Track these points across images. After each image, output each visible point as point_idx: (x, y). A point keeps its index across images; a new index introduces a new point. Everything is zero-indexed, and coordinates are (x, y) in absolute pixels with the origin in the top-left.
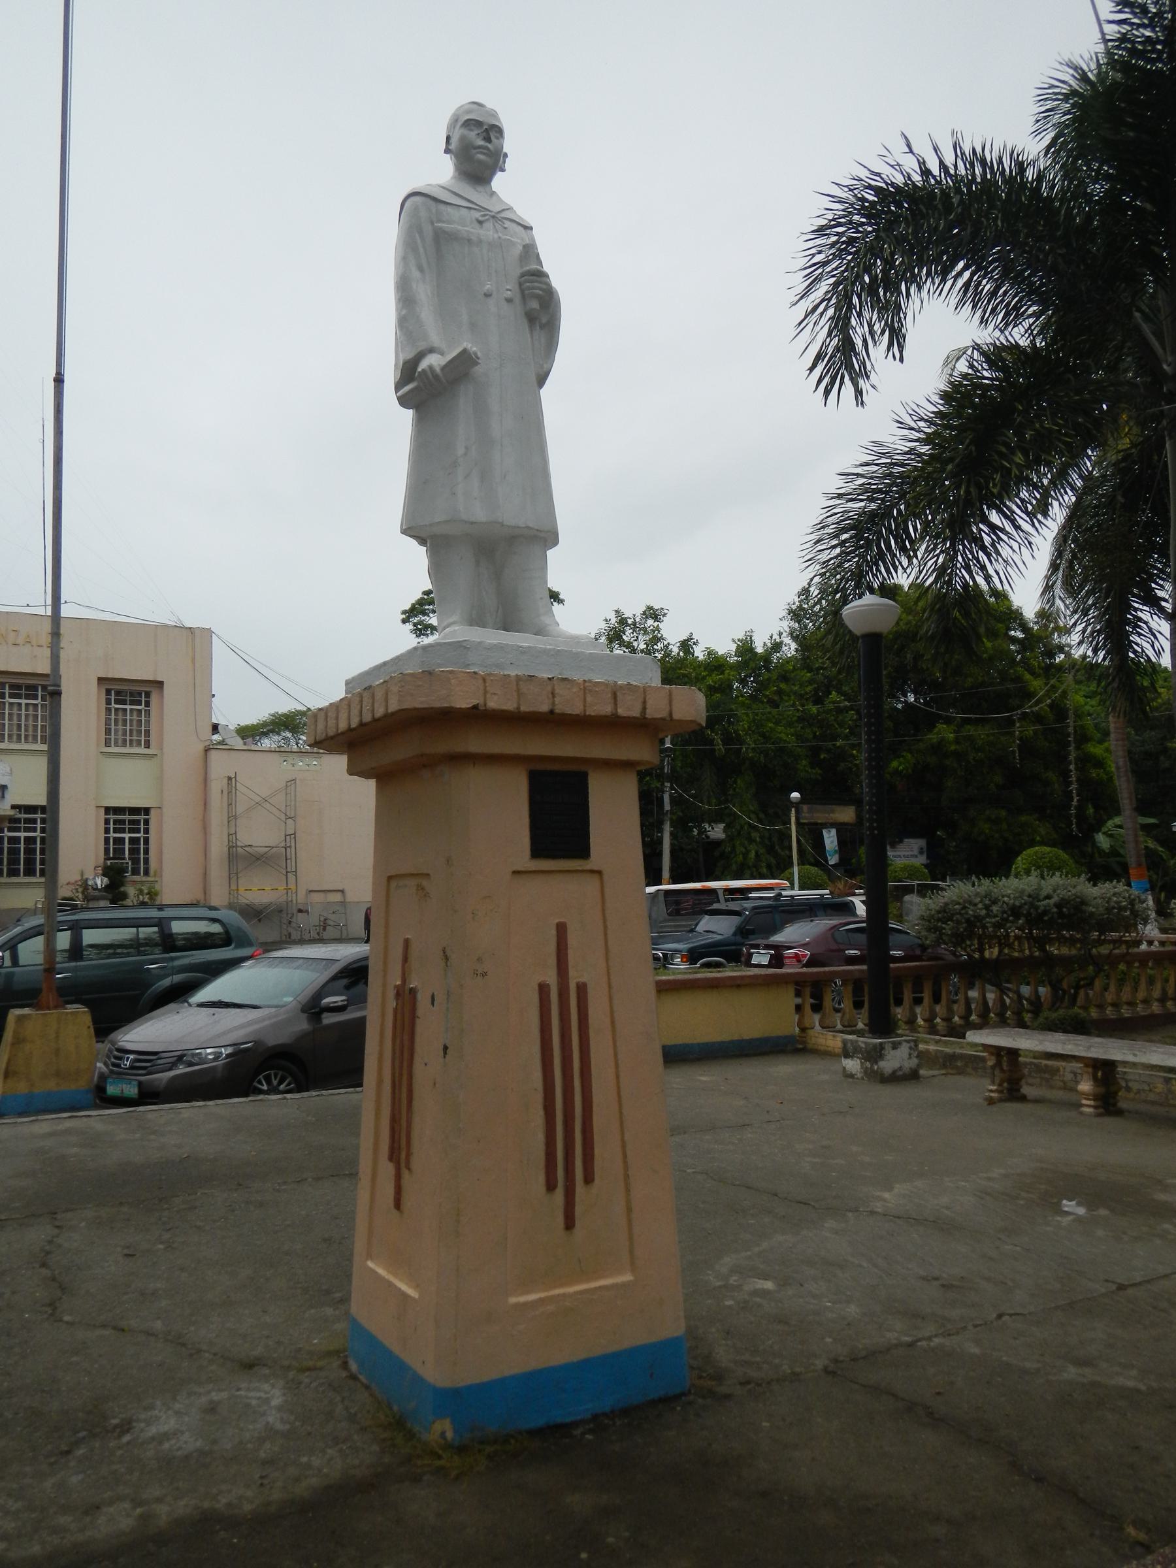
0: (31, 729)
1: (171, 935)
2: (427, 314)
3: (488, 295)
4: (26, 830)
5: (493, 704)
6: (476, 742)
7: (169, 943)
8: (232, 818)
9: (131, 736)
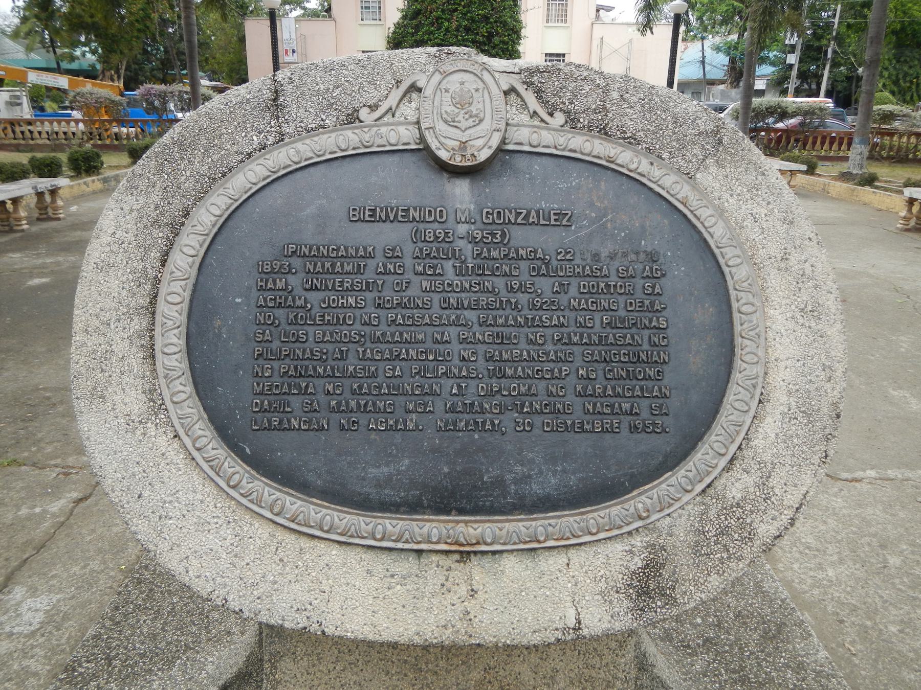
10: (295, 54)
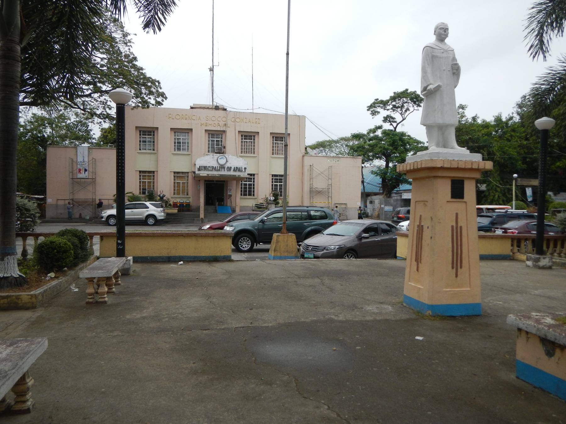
1: (311, 215)
2: (429, 75)
3: (444, 70)
5: (445, 166)
6: (440, 174)
7: (310, 217)
8: (311, 179)
10: (87, 173)
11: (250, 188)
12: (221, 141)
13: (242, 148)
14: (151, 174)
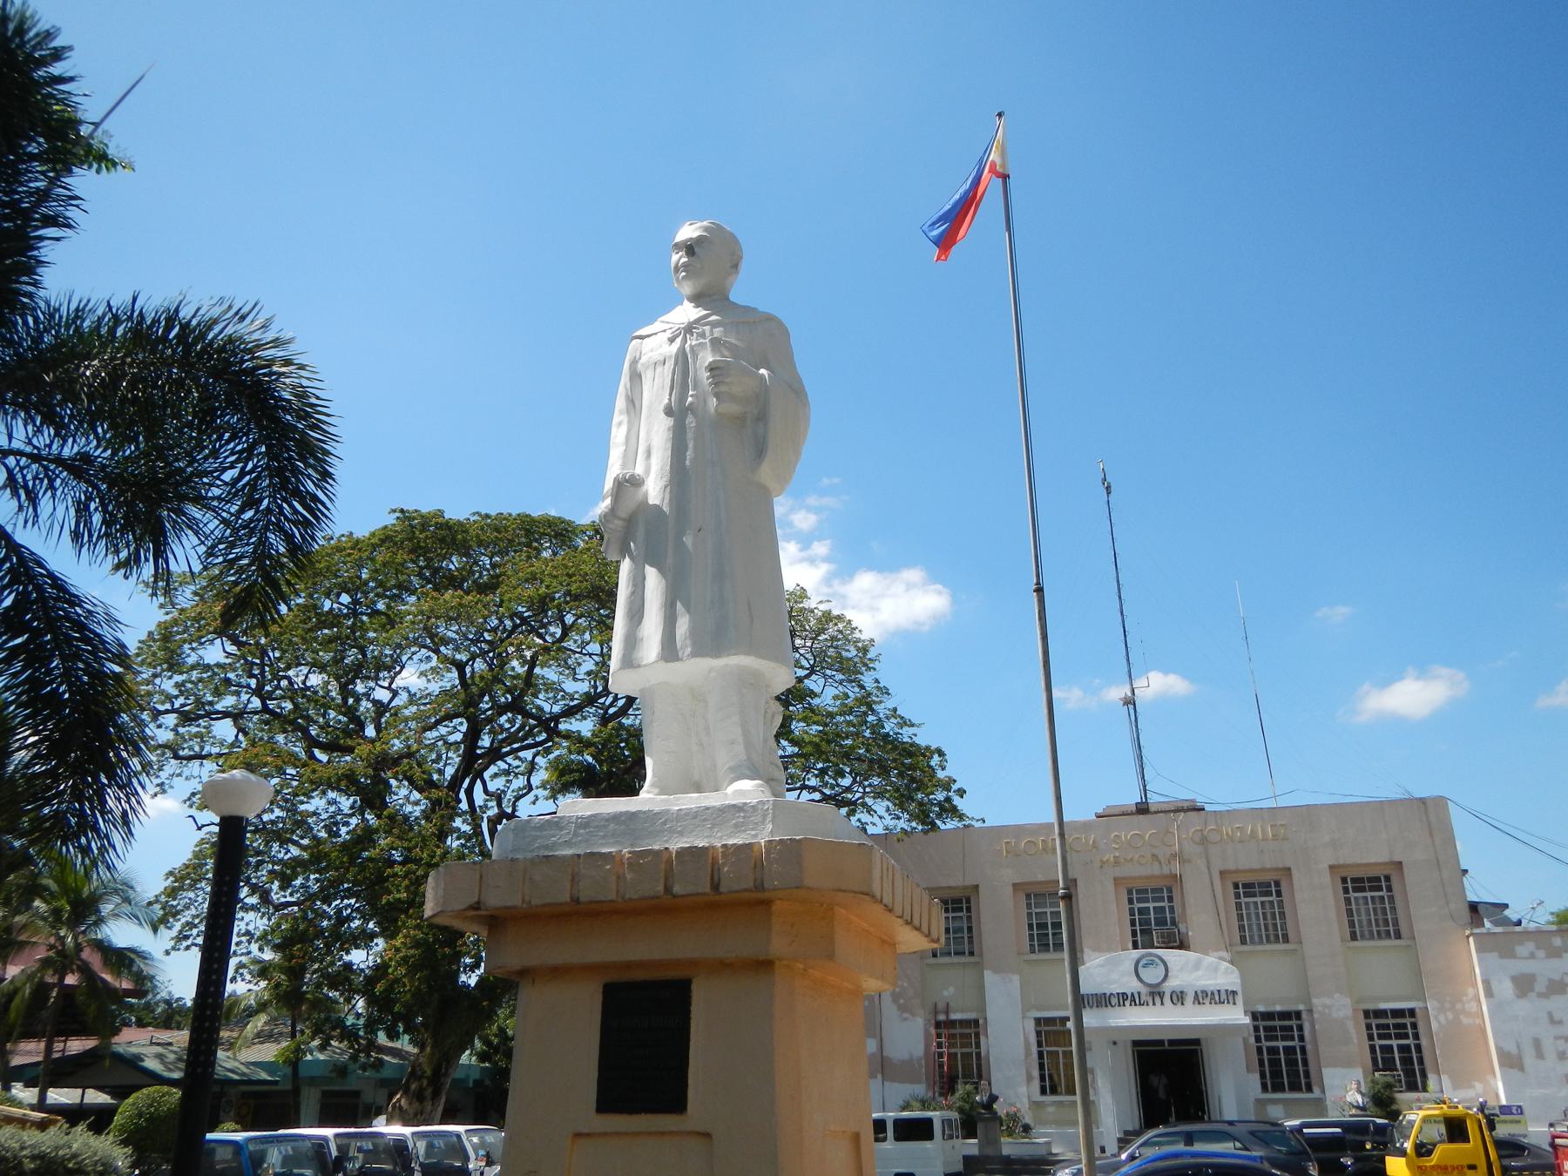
0: (1271, 928)
4: (1284, 1038)
9: (1377, 925)
11: (1292, 1063)
12: (1172, 909)
13: (1241, 928)
14: (968, 1031)
